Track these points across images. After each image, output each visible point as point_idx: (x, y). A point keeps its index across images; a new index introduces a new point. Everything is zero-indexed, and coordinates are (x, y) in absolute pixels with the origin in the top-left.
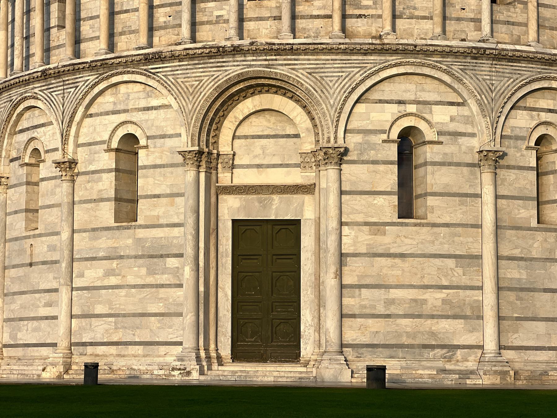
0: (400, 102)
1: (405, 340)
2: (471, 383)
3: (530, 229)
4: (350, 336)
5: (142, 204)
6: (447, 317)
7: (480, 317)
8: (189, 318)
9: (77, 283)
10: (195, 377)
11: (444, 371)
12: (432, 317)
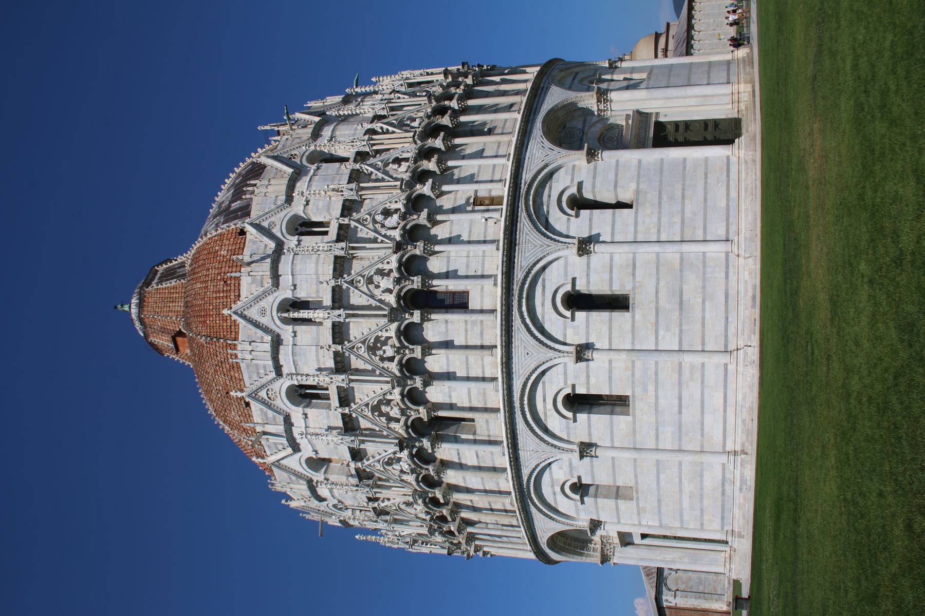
0: (554, 494)
1: (719, 503)
3: (634, 422)
6: (702, 481)
11: (741, 489)
12: (702, 489)
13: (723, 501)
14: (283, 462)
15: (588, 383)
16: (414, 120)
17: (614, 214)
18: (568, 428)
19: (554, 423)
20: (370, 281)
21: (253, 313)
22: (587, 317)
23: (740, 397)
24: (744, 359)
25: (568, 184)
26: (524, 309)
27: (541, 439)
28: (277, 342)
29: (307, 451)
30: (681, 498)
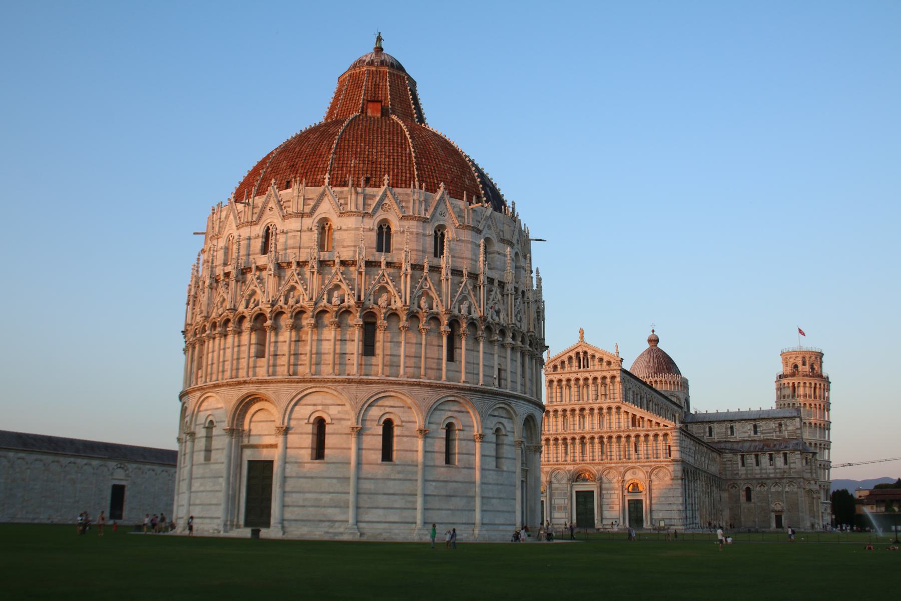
0: (314, 405)
1: (311, 518)
2: (337, 538)
4: (288, 516)
5: (213, 453)
6: (332, 507)
7: (348, 507)
8: (222, 507)
9: (193, 489)
10: (222, 534)
11: (327, 533)
12: (324, 507)
13: (314, 521)
14: (326, 199)
15: (403, 436)
18: (372, 420)
19: (375, 412)
20: (465, 298)
21: (442, 207)
23: (396, 531)
26: (450, 398)
27: (366, 402)
29: (336, 222)
30: (315, 492)
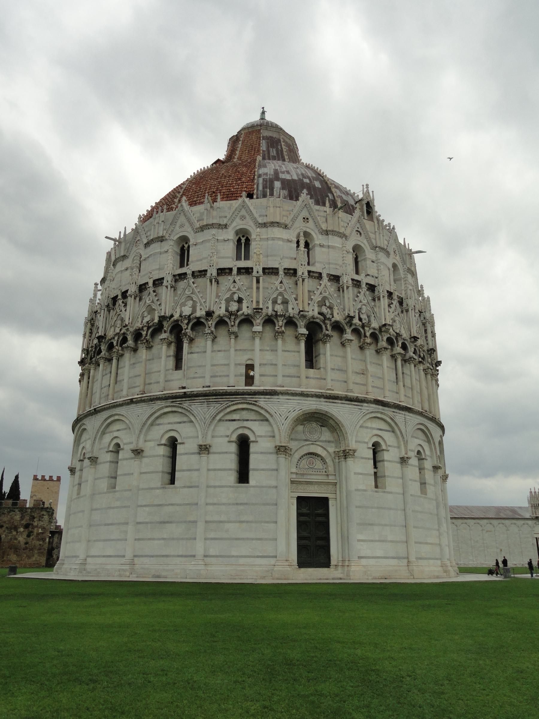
3: (103, 493)
15: (124, 459)
16: (331, 308)
17: (230, 470)
19: (107, 438)
21: (182, 219)
22: (160, 456)
24: (123, 570)
25: (257, 434)
28: (161, 239)
